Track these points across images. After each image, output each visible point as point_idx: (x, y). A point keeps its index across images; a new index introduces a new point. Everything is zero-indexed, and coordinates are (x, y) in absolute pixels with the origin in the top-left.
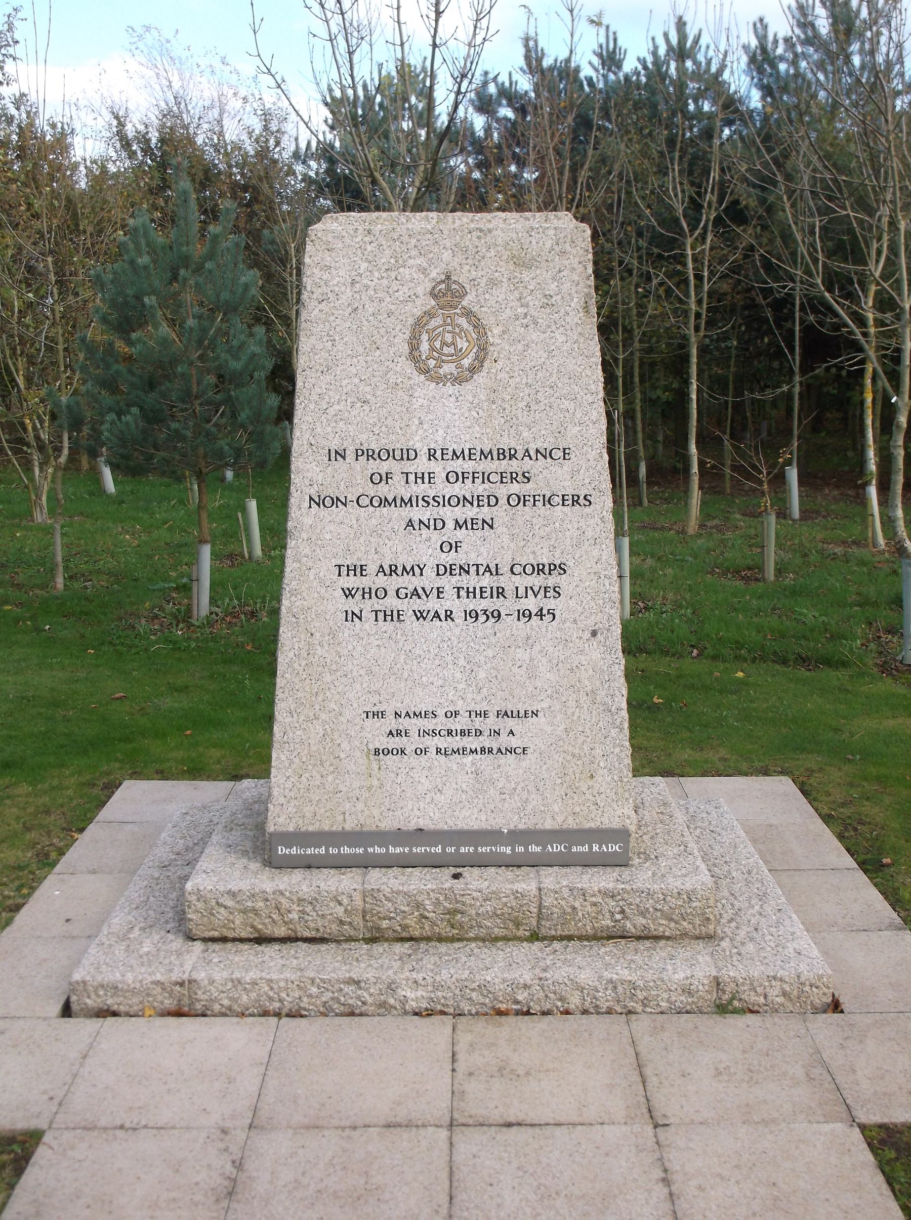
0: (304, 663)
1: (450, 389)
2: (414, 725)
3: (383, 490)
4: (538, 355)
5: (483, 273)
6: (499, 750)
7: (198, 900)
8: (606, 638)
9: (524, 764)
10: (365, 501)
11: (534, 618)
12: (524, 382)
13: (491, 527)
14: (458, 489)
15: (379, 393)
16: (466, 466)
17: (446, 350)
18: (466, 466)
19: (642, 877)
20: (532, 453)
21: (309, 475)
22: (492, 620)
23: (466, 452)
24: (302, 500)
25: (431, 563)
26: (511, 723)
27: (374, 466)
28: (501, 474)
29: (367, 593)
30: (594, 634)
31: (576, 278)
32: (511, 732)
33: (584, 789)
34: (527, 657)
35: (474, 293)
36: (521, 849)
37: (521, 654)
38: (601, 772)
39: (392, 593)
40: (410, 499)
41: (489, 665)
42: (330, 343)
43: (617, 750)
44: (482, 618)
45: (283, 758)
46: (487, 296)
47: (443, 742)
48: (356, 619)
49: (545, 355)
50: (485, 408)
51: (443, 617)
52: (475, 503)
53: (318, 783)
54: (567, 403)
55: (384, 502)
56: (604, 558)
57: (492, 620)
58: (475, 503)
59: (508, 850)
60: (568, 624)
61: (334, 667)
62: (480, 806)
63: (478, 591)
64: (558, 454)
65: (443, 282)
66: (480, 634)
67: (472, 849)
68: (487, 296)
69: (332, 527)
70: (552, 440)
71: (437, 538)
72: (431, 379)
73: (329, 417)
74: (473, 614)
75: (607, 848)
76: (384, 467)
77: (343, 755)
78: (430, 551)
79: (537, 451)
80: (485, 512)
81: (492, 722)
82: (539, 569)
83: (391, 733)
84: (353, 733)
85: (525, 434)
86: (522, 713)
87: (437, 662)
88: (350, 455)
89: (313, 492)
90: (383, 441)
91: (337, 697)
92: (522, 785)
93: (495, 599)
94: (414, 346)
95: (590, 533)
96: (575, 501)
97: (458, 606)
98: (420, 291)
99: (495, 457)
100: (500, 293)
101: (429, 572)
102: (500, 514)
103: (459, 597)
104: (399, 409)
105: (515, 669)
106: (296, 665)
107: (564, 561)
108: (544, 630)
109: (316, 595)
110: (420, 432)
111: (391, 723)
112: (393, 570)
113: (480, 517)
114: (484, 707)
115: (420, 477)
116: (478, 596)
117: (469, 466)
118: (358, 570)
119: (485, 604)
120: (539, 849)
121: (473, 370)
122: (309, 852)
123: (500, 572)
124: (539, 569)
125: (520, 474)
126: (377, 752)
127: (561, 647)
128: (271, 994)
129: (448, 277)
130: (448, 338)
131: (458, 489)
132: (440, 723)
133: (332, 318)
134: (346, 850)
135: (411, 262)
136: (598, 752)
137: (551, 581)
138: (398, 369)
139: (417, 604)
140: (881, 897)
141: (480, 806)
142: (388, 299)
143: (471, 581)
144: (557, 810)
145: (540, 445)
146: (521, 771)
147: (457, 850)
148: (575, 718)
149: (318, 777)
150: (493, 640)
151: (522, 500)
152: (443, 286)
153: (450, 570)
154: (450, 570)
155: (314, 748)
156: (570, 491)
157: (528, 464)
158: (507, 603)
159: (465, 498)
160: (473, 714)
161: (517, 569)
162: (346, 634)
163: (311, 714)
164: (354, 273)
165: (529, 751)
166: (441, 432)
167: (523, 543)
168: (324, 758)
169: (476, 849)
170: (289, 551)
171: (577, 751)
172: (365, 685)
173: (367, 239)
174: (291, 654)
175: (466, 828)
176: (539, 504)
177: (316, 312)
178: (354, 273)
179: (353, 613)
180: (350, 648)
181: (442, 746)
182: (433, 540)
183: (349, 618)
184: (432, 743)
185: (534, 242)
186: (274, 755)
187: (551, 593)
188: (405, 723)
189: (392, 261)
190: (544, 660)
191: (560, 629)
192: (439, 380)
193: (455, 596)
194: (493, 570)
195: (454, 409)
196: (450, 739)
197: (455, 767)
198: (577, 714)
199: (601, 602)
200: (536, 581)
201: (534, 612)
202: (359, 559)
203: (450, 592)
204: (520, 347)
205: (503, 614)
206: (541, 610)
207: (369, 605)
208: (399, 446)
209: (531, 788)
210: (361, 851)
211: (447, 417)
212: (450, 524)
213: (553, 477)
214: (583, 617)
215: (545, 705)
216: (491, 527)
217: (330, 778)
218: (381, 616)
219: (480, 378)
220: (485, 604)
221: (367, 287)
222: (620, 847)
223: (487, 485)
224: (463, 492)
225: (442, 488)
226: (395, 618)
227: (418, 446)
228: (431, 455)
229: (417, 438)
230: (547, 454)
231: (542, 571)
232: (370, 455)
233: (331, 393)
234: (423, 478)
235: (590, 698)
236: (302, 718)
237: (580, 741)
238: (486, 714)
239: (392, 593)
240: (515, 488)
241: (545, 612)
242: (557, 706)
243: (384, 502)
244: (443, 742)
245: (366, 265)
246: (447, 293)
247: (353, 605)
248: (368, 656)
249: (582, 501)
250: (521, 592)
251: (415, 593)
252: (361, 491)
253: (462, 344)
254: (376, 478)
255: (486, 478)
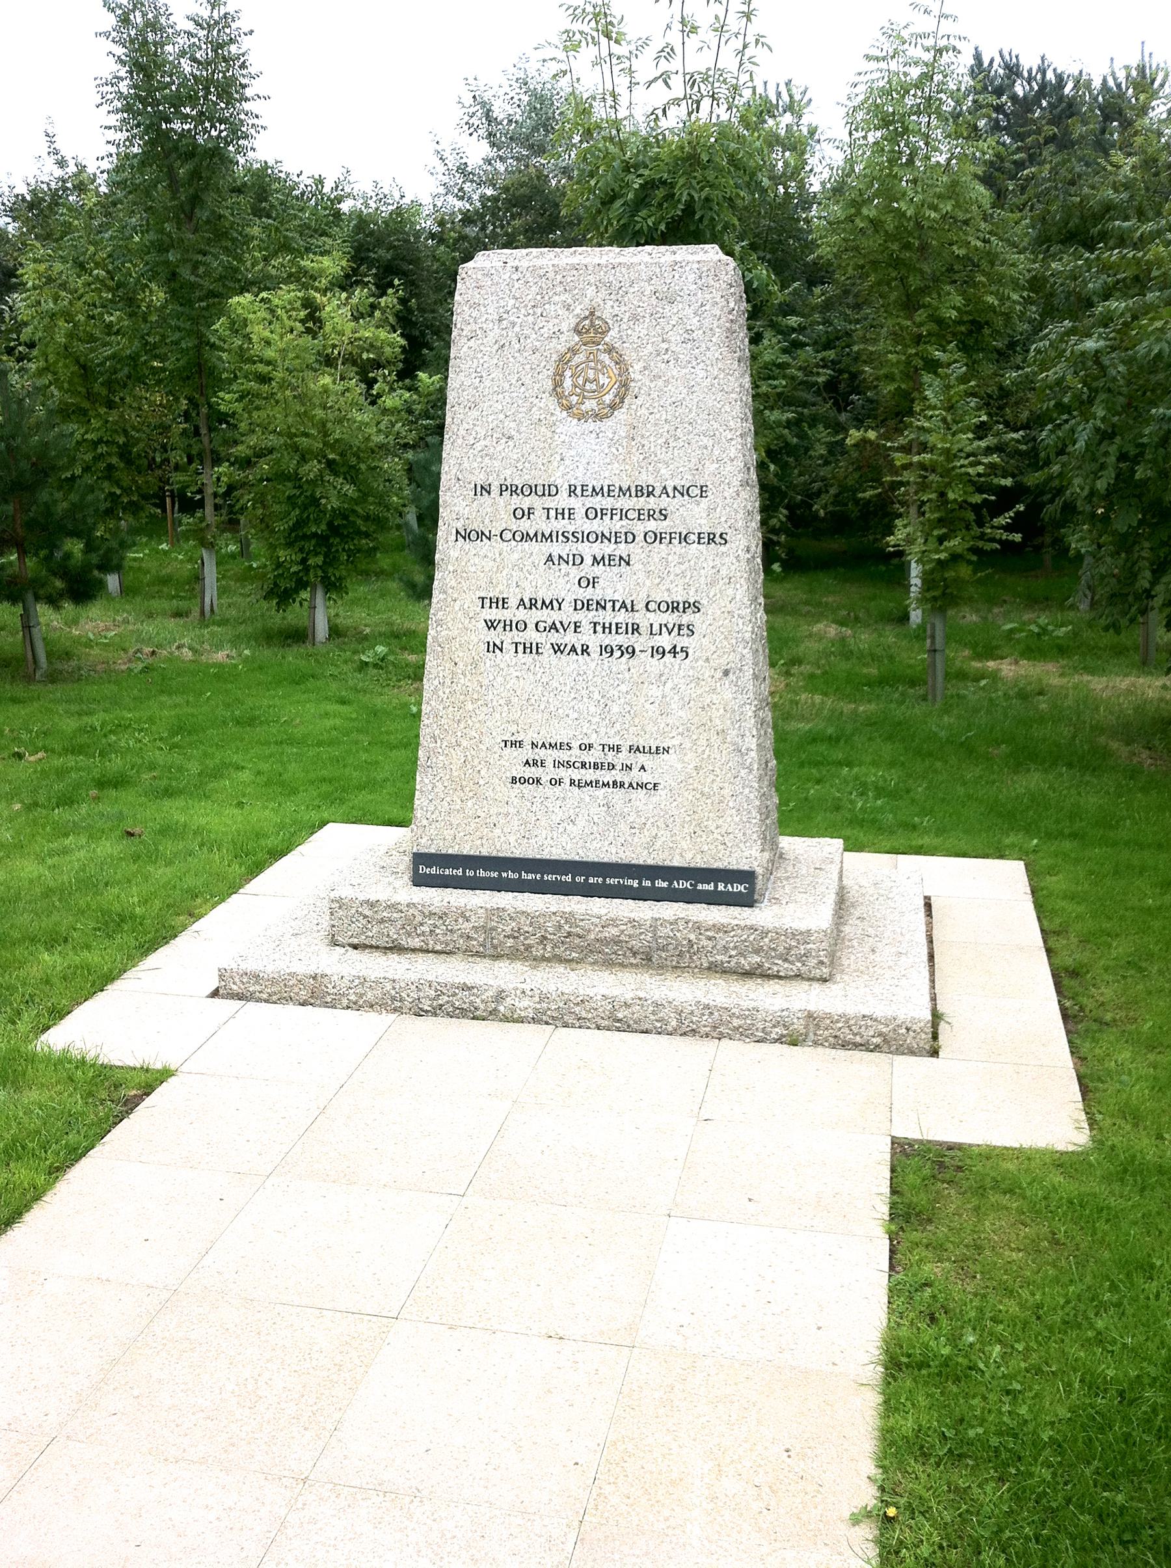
0: (447, 691)
1: (591, 425)
2: (550, 755)
3: (525, 525)
4: (677, 390)
5: (626, 308)
6: (631, 785)
7: (340, 908)
8: (738, 678)
9: (654, 799)
10: (508, 535)
11: (668, 655)
12: (664, 417)
13: (628, 564)
14: (596, 526)
15: (523, 429)
16: (604, 502)
17: (588, 386)
18: (604, 502)
19: (761, 916)
20: (670, 490)
21: (456, 509)
22: (626, 656)
23: (606, 489)
24: (449, 533)
25: (569, 598)
26: (642, 759)
27: (516, 501)
28: (636, 510)
29: (508, 626)
30: (726, 673)
31: (718, 313)
32: (643, 767)
33: (712, 828)
34: (659, 694)
35: (617, 329)
36: (648, 883)
37: (655, 692)
38: (729, 812)
39: (531, 626)
40: (551, 535)
41: (622, 700)
42: (478, 380)
43: (747, 790)
44: (617, 654)
45: (427, 781)
46: (629, 332)
47: (576, 774)
48: (497, 650)
49: (685, 391)
50: (625, 444)
51: (579, 652)
52: (613, 540)
53: (458, 807)
54: (705, 440)
55: (526, 537)
56: (738, 597)
57: (626, 656)
58: (613, 540)
59: (635, 884)
60: (700, 662)
61: (475, 696)
62: (611, 838)
63: (614, 627)
64: (695, 491)
65: (586, 318)
66: (614, 669)
67: (600, 880)
68: (629, 332)
69: (477, 560)
70: (690, 478)
71: (575, 573)
72: (574, 416)
73: (476, 452)
74: (609, 649)
75: (735, 887)
76: (526, 503)
77: (482, 782)
78: (568, 586)
79: (675, 488)
80: (622, 549)
81: (624, 757)
82: (673, 607)
83: (527, 762)
84: (491, 761)
85: (663, 471)
86: (654, 750)
87: (573, 695)
88: (495, 490)
89: (459, 525)
90: (527, 477)
91: (478, 725)
92: (652, 820)
93: (630, 635)
94: (558, 384)
95: (724, 572)
96: (711, 540)
97: (594, 641)
98: (564, 327)
99: (633, 494)
100: (641, 329)
101: (567, 607)
102: (636, 550)
103: (595, 632)
104: (542, 445)
105: (647, 706)
106: (440, 693)
107: (698, 599)
108: (677, 667)
109: (461, 626)
110: (562, 468)
111: (527, 753)
112: (533, 604)
113: (617, 553)
114: (615, 741)
115: (560, 513)
116: (614, 631)
117: (608, 503)
118: (500, 603)
119: (621, 639)
120: (665, 885)
121: (613, 407)
122: (447, 873)
123: (636, 608)
124: (673, 607)
125: (657, 511)
126: (514, 780)
127: (693, 685)
128: (393, 992)
129: (592, 314)
130: (591, 374)
131: (596, 526)
132: (575, 755)
133: (480, 355)
134: (482, 873)
135: (556, 298)
136: (726, 792)
137: (685, 619)
138: (542, 405)
139: (554, 637)
140: (422, 780)
141: (611, 838)
142: (534, 336)
143: (606, 616)
144: (686, 847)
145: (678, 482)
146: (651, 807)
147: (586, 880)
148: (705, 756)
149: (459, 802)
150: (627, 675)
151: (658, 537)
152: (587, 322)
153: (587, 605)
154: (587, 605)
155: (455, 774)
156: (706, 529)
157: (664, 501)
158: (641, 639)
159: (603, 535)
160: (607, 748)
161: (652, 606)
162: (488, 665)
163: (454, 741)
164: (501, 310)
165: (660, 787)
166: (581, 468)
167: (658, 580)
168: (464, 783)
169: (605, 880)
170: (436, 583)
171: (706, 790)
172: (504, 715)
173: (515, 277)
174: (436, 682)
175: (596, 860)
176: (675, 542)
177: (465, 349)
178: (501, 310)
179: (495, 645)
180: (491, 678)
181: (576, 777)
182: (571, 576)
183: (491, 649)
184: (565, 774)
185: (677, 277)
186: (418, 778)
187: (685, 631)
188: (542, 753)
189: (539, 297)
190: (676, 698)
191: (693, 668)
192: (582, 417)
193: (592, 631)
194: (629, 606)
195: (603, 444)
196: (583, 771)
197: (587, 799)
198: (707, 752)
199: (734, 641)
200: (671, 618)
201: (667, 650)
202: (501, 592)
203: (586, 627)
204: (660, 383)
205: (637, 650)
206: (675, 647)
207: (509, 637)
208: (541, 482)
209: (661, 824)
210: (496, 875)
211: (586, 453)
212: (588, 560)
213: (692, 515)
214: (715, 656)
215: (676, 742)
216: (628, 564)
217: (470, 803)
218: (520, 648)
219: (621, 415)
220: (621, 639)
221: (514, 324)
222: (745, 888)
223: (625, 522)
224: (601, 529)
225: (581, 524)
226: (534, 651)
227: (559, 482)
228: (572, 491)
229: (559, 474)
230: (685, 492)
231: (677, 608)
232: (514, 490)
233: (476, 428)
234: (563, 514)
235: (720, 737)
236: (445, 743)
237: (709, 780)
238: (618, 749)
239: (531, 626)
240: (652, 525)
241: (678, 649)
242: (688, 744)
243: (526, 537)
244: (576, 774)
245: (513, 301)
246: (591, 329)
247: (494, 636)
248: (508, 687)
249: (717, 539)
250: (656, 628)
251: (553, 627)
252: (504, 526)
253: (603, 380)
254: (519, 513)
255: (624, 515)
